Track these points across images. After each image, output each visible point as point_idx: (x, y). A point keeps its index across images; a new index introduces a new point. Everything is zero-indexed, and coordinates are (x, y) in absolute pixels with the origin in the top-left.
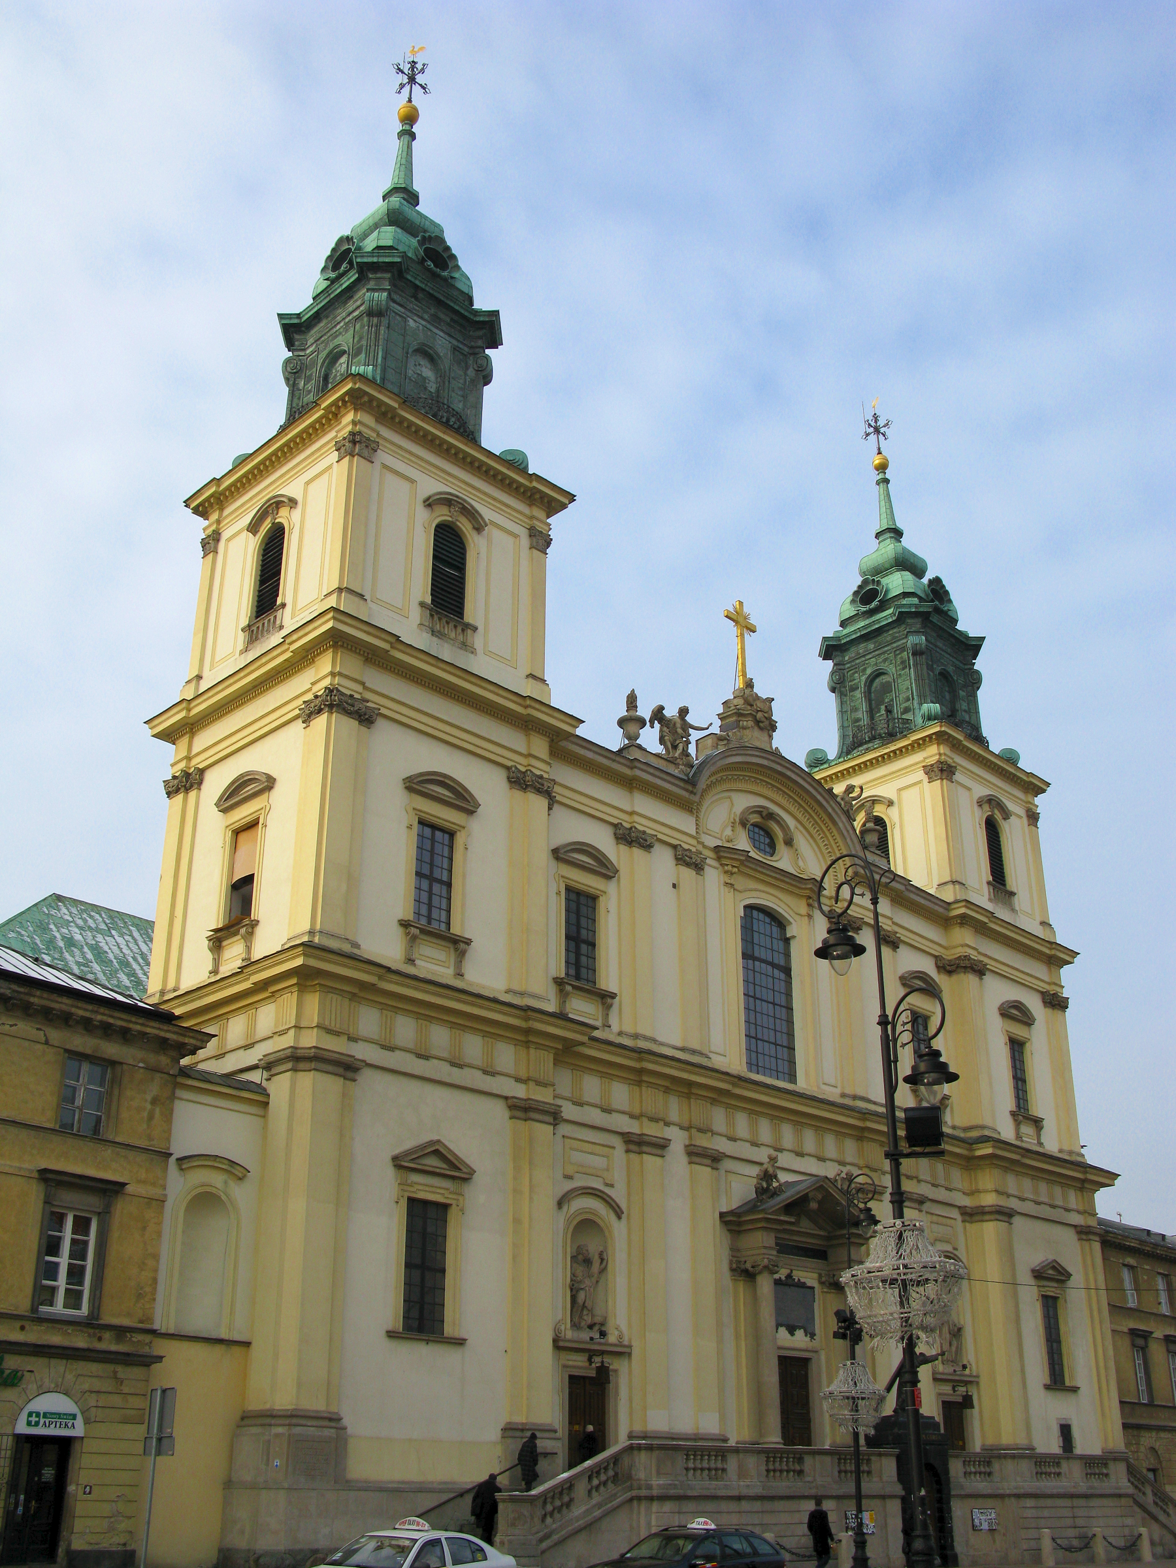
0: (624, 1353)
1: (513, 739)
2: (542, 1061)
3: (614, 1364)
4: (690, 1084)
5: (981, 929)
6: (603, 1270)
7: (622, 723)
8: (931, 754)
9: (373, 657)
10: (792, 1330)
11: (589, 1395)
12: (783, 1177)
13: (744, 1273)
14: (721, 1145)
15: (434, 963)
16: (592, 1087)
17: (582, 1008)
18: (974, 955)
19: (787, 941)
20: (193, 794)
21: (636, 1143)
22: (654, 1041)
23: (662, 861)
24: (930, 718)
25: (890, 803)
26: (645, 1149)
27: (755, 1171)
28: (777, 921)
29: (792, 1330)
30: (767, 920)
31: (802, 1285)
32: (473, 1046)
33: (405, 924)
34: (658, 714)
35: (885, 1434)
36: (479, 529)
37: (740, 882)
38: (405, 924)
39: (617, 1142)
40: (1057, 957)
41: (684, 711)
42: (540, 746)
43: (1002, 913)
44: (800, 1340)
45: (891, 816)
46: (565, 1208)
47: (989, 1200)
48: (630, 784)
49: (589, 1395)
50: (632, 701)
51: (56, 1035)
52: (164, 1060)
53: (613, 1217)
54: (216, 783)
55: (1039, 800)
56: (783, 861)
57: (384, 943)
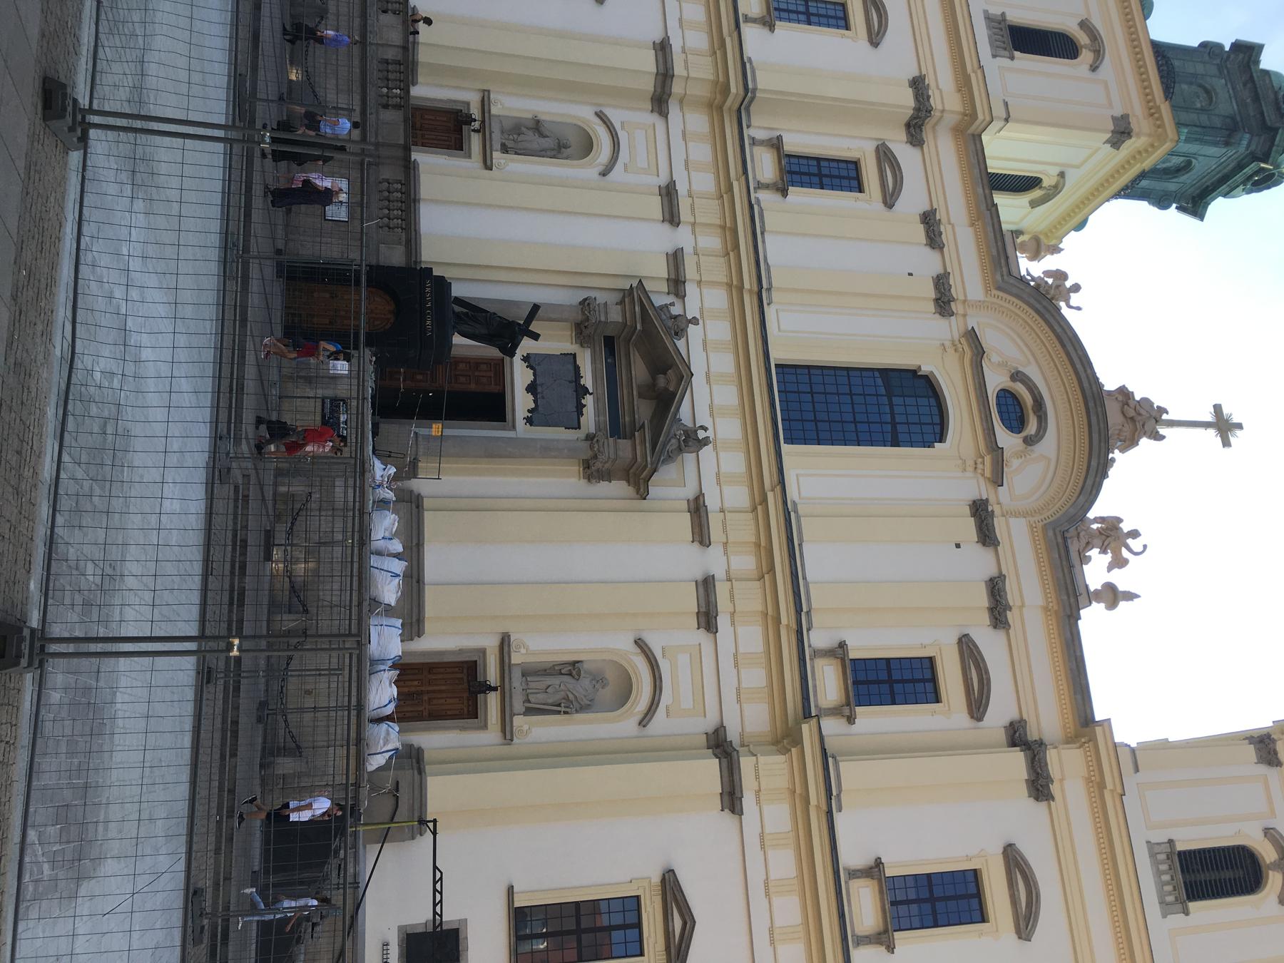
4: (736, 247)
10: (531, 388)
11: (450, 129)
12: (681, 344)
14: (691, 289)
21: (669, 193)
22: (762, 233)
23: (930, 263)
26: (666, 199)
27: (676, 310)
29: (531, 388)
30: (936, 419)
31: (580, 408)
34: (1061, 276)
36: (1094, 68)
41: (1076, 288)
44: (522, 402)
46: (598, 121)
49: (450, 129)
53: (601, 168)
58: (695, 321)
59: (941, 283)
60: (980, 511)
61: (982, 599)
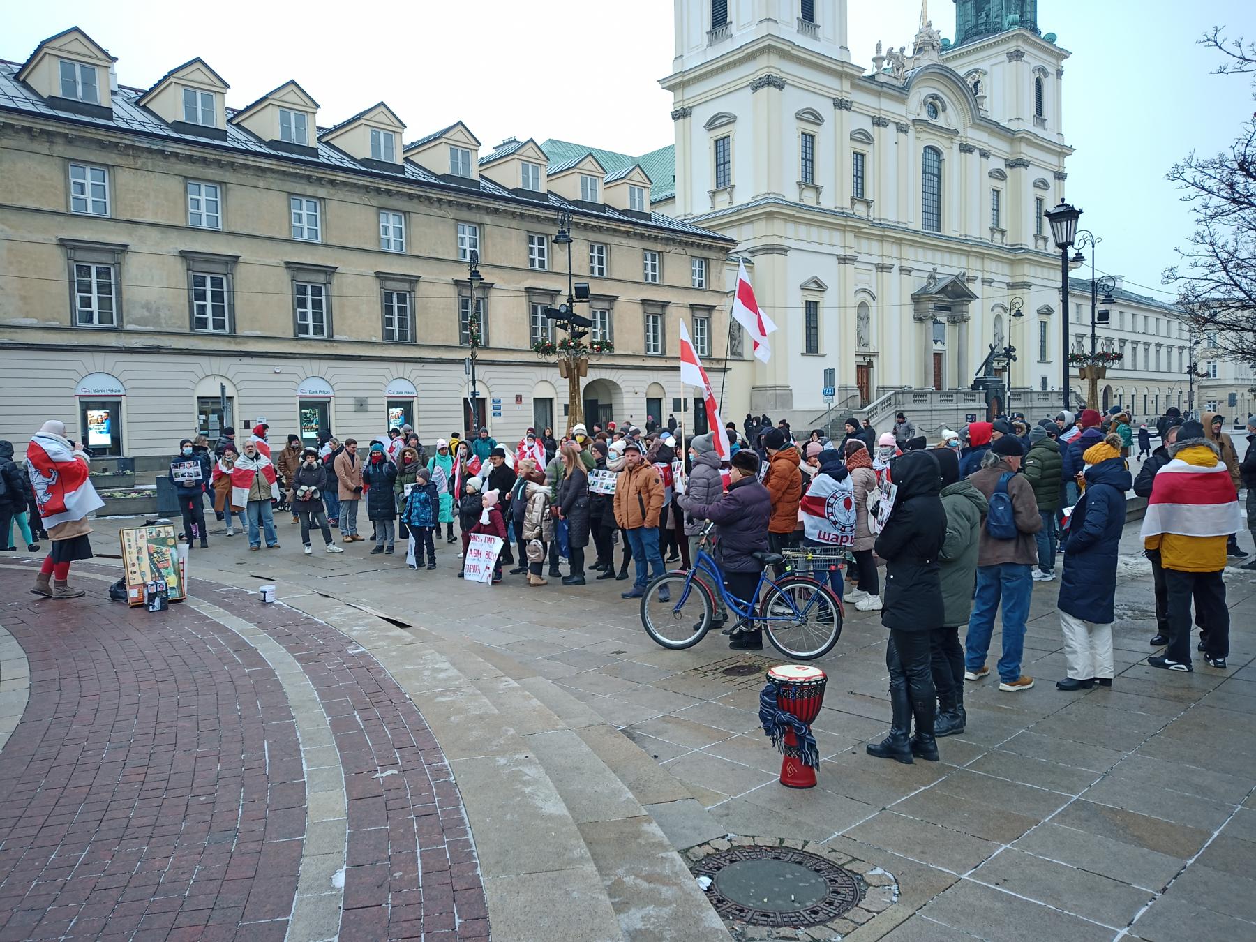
0: (875, 355)
1: (832, 82)
2: (850, 238)
3: (874, 360)
5: (1030, 143)
6: (868, 322)
7: (874, 60)
8: (1012, 46)
9: (785, 55)
10: (936, 342)
11: (864, 370)
13: (920, 319)
15: (809, 198)
16: (865, 245)
17: (860, 210)
18: (1025, 158)
19: (940, 161)
20: (688, 119)
24: (1013, 23)
25: (986, 73)
28: (937, 152)
29: (936, 342)
32: (825, 235)
33: (799, 184)
34: (890, 51)
35: (977, 384)
37: (923, 136)
38: (799, 184)
39: (873, 268)
40: (1063, 151)
41: (902, 50)
42: (846, 85)
43: (1039, 131)
44: (938, 346)
45: (984, 80)
47: (1019, 280)
48: (879, 95)
50: (879, 47)
51: (690, 251)
52: (721, 255)
54: (702, 115)
55: (1065, 63)
56: (940, 121)
57: (792, 195)
58: (935, 270)
59: (902, 129)
60: (966, 149)
61: (984, 160)
